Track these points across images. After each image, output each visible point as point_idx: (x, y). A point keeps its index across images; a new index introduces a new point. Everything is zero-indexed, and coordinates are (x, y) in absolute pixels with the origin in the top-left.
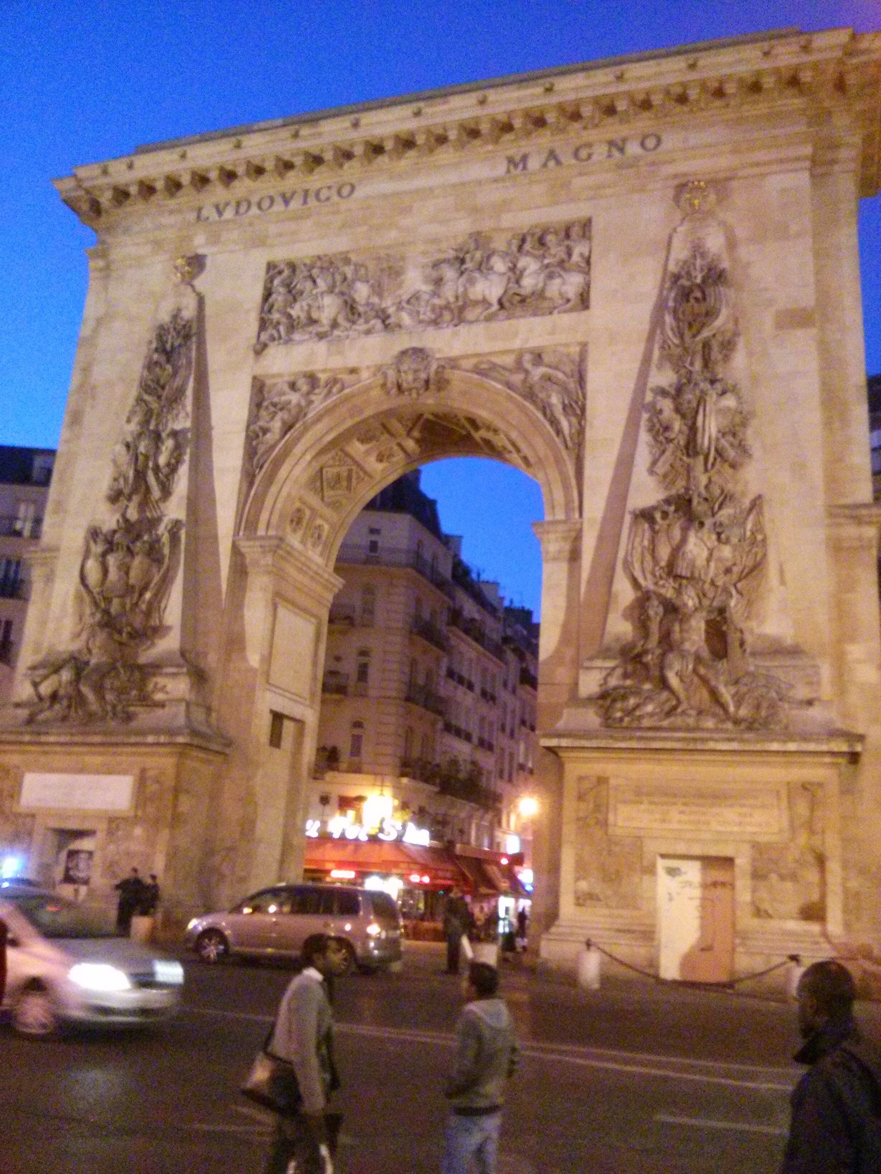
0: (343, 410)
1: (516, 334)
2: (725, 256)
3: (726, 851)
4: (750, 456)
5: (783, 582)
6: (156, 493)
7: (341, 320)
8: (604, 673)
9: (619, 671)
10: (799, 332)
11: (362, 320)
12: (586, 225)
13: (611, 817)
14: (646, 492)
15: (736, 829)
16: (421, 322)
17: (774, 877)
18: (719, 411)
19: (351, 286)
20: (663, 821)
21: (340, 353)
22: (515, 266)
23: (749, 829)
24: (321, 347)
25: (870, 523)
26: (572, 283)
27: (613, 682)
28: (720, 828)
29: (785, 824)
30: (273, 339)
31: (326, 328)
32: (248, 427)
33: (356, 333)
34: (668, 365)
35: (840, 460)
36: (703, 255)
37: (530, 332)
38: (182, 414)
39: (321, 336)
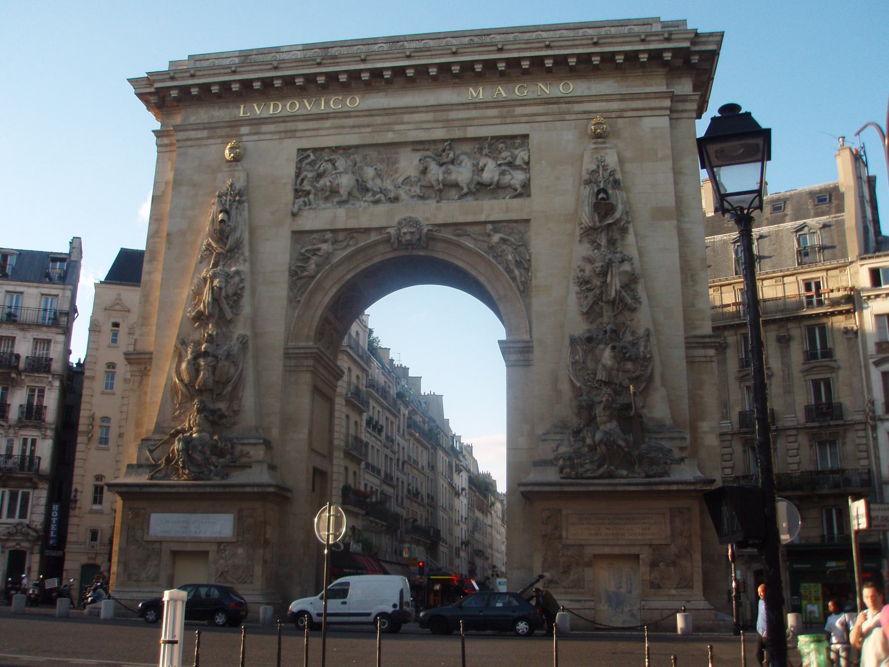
2: (618, 169)
3: (635, 550)
4: (640, 303)
6: (229, 315)
7: (356, 193)
8: (556, 444)
11: (370, 194)
12: (526, 137)
13: (564, 534)
15: (640, 537)
16: (413, 197)
17: (662, 565)
18: (620, 274)
19: (361, 168)
20: (597, 534)
22: (478, 163)
23: (648, 537)
24: (341, 212)
25: (710, 347)
26: (518, 177)
28: (631, 537)
29: (669, 532)
30: (305, 204)
31: (345, 197)
32: (290, 268)
33: (366, 204)
34: (585, 240)
36: (605, 168)
37: (492, 209)
38: (242, 258)
39: (342, 203)
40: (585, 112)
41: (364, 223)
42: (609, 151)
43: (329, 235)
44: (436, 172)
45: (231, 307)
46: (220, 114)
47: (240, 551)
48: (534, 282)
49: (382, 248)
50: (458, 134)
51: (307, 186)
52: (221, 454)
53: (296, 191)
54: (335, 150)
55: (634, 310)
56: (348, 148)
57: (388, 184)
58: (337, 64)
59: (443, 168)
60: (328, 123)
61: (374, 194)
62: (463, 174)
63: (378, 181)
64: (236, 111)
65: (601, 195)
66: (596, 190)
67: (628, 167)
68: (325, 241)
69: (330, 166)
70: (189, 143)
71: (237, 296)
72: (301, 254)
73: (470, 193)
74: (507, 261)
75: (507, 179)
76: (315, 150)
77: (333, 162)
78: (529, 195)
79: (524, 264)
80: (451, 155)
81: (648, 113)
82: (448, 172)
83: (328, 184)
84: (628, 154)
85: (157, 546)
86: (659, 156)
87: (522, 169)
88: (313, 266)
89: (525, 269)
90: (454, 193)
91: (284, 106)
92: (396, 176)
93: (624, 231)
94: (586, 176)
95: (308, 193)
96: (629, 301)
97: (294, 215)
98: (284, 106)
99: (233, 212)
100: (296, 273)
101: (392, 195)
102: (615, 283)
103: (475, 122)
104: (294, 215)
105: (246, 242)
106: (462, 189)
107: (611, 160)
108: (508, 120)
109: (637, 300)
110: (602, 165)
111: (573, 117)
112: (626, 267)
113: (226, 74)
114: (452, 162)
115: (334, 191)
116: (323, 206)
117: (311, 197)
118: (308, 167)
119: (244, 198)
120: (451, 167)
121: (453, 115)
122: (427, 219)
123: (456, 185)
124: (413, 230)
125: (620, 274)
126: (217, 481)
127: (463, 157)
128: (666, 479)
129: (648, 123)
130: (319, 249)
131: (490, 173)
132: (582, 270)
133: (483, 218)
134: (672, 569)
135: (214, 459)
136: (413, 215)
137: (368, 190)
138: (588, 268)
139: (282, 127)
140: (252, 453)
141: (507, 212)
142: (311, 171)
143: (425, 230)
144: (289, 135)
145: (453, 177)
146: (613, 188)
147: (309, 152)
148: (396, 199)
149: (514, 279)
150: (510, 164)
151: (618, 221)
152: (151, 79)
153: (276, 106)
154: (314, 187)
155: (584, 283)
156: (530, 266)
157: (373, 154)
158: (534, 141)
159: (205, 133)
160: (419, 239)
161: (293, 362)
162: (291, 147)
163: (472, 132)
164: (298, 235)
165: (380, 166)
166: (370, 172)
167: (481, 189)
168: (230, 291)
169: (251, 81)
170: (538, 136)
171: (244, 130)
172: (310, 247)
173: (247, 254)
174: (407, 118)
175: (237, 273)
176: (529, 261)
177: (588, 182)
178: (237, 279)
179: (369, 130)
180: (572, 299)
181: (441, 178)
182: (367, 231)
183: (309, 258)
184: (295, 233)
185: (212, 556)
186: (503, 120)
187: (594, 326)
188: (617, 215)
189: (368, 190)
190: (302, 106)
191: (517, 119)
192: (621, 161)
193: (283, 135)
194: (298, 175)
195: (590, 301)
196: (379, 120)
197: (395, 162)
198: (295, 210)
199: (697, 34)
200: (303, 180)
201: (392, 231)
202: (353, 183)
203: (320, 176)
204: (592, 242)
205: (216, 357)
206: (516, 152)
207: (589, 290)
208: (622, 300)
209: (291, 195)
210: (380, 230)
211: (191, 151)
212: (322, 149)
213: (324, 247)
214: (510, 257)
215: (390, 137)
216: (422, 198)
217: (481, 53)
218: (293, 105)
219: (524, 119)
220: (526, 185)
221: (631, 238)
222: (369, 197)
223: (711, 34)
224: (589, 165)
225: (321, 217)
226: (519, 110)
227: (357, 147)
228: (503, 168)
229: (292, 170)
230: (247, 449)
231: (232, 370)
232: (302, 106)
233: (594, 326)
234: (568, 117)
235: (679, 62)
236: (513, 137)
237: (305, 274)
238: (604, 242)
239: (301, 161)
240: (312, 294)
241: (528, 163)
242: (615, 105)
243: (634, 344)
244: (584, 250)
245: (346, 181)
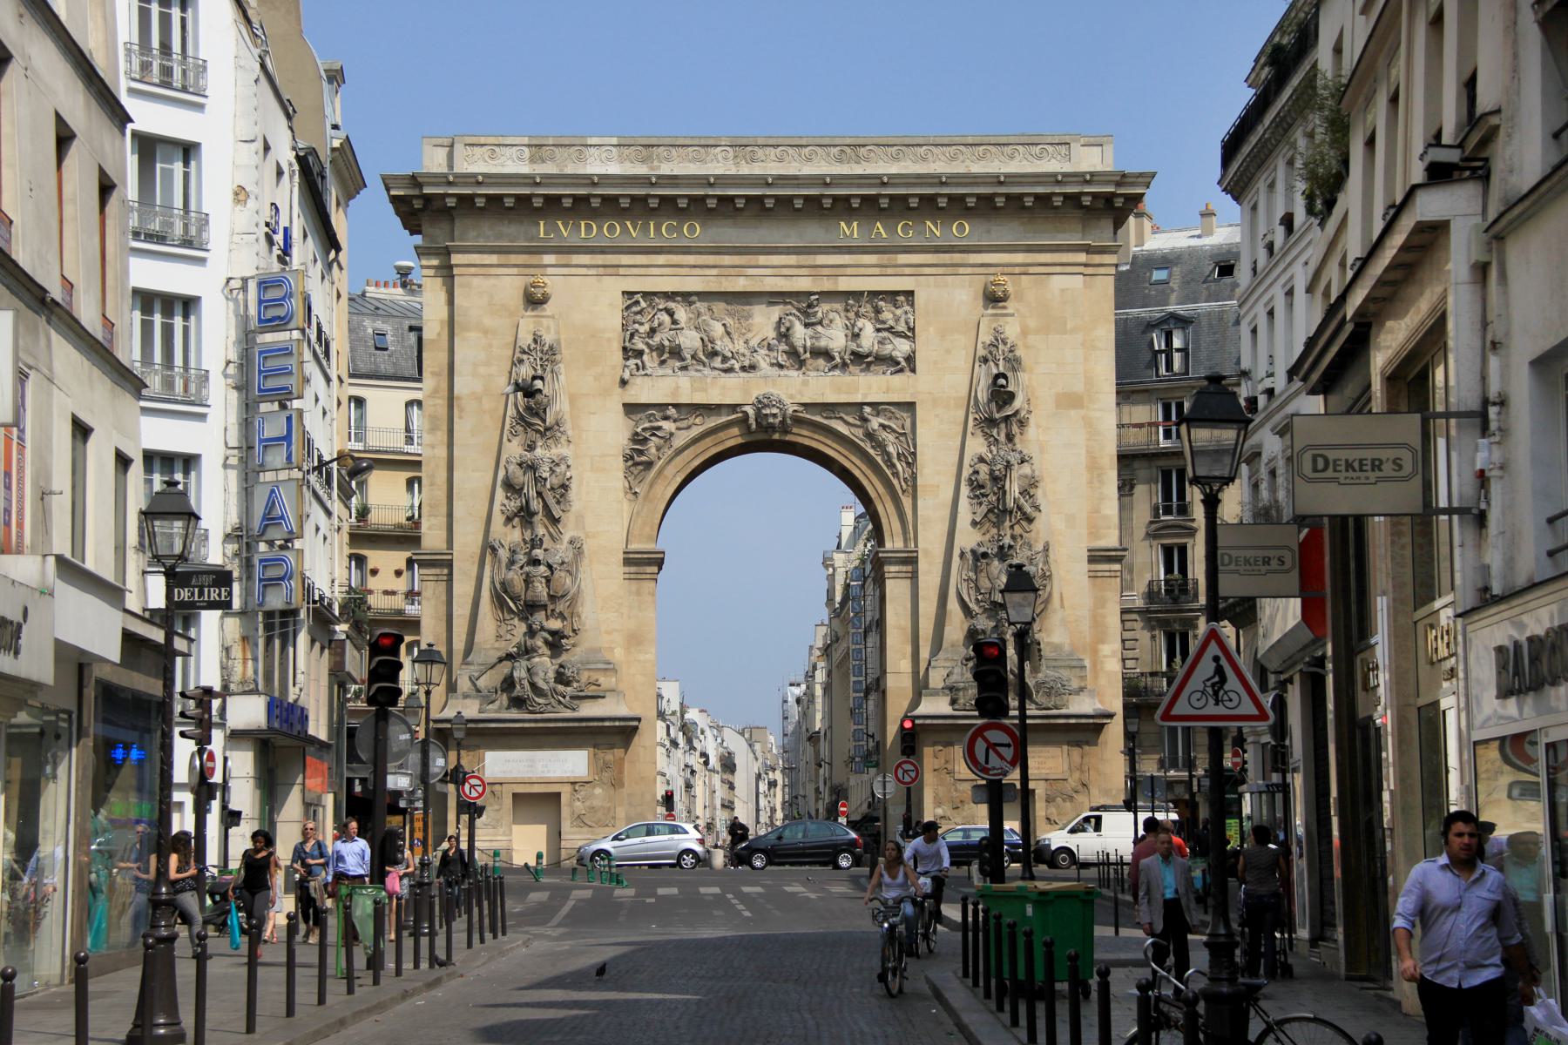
0: (708, 441)
1: (857, 390)
5: (1062, 606)
6: (557, 513)
9: (957, 670)
10: (1073, 413)
11: (719, 359)
12: (911, 293)
14: (968, 538)
16: (772, 365)
21: (705, 390)
22: (853, 326)
27: (954, 678)
29: (1066, 766)
34: (979, 432)
35: (1098, 511)
40: (982, 265)
41: (715, 399)
42: (1009, 319)
43: (672, 411)
44: (800, 334)
45: (558, 502)
46: (513, 232)
47: (598, 791)
48: (919, 481)
49: (735, 431)
50: (827, 285)
51: (641, 346)
52: (567, 683)
53: (625, 349)
54: (670, 296)
55: (1030, 520)
56: (690, 294)
57: (739, 346)
58: (676, 186)
59: (810, 331)
60: (661, 259)
61: (725, 359)
62: (835, 338)
63: (726, 339)
64: (534, 229)
65: (1002, 381)
66: (995, 371)
67: (1031, 339)
68: (666, 418)
69: (666, 318)
70: (473, 270)
71: (565, 487)
72: (637, 434)
73: (844, 366)
74: (889, 454)
75: (887, 349)
76: (646, 295)
77: (671, 313)
78: (913, 371)
79: (910, 458)
80: (820, 315)
81: (1058, 269)
82: (816, 337)
83: (666, 343)
84: (1032, 323)
85: (497, 787)
86: (1069, 326)
87: (906, 337)
88: (653, 450)
89: (908, 464)
90: (821, 362)
91: (600, 228)
92: (749, 335)
93: (1022, 424)
94: (981, 352)
95: (640, 354)
96: (1028, 509)
97: (623, 383)
98: (600, 228)
99: (548, 377)
100: (632, 458)
101: (747, 363)
102: (1014, 489)
103: (849, 271)
104: (623, 383)
105: (567, 417)
106: (833, 358)
107: (1011, 330)
108: (889, 271)
109: (1037, 508)
110: (998, 340)
111: (969, 270)
112: (1026, 469)
113: (526, 185)
114: (820, 323)
115: (676, 353)
116: (661, 372)
117: (645, 357)
118: (638, 317)
119: (558, 357)
120: (819, 328)
121: (822, 259)
122: (791, 397)
123: (826, 354)
124: (775, 411)
125: (1021, 477)
126: (568, 714)
127: (832, 315)
128: (1064, 711)
129: (1058, 282)
130: (659, 428)
131: (869, 340)
132: (977, 472)
133: (859, 400)
134: (1068, 804)
135: (560, 688)
136: (775, 391)
137: (714, 354)
138: (984, 469)
139: (599, 259)
140: (602, 680)
141: (887, 391)
142: (642, 324)
143: (790, 411)
144: (610, 271)
145: (823, 343)
146: (1014, 370)
147: (638, 297)
148: (753, 367)
149: (896, 474)
150: (890, 329)
151: (1017, 412)
152: (414, 180)
153: (589, 227)
154: (647, 344)
155: (976, 486)
156: (915, 459)
157: (719, 307)
158: (919, 299)
159: (493, 259)
160: (783, 422)
161: (633, 569)
162: (614, 287)
163: (845, 284)
164: (631, 409)
165: (729, 321)
166: (717, 329)
167: (859, 359)
168: (556, 481)
169: (559, 198)
170: (926, 292)
171: (549, 259)
172: (647, 425)
173: (570, 433)
174: (762, 260)
175: (564, 459)
176: (914, 454)
177: (985, 360)
178: (563, 467)
179: (714, 272)
180: (964, 503)
181: (808, 344)
182: (719, 406)
183: (646, 440)
184: (625, 405)
185: (564, 799)
186: (883, 270)
187: (988, 536)
188: (1018, 403)
189: (714, 354)
190: (625, 230)
191: (899, 271)
192: (1025, 332)
193: (601, 271)
194: (624, 327)
195: (984, 509)
196: (727, 260)
197: (749, 316)
198: (627, 376)
199: (1124, 176)
200: (632, 336)
201: (750, 411)
202: (698, 344)
203: (653, 331)
204: (987, 436)
205: (550, 567)
206: (898, 312)
207: (983, 495)
208: (1020, 508)
209: (620, 353)
210: (733, 408)
211: (475, 281)
212: (655, 294)
213: (668, 426)
214: (891, 449)
215: (740, 285)
216: (781, 366)
217: (860, 186)
218: (611, 229)
219: (908, 271)
220: (910, 359)
221: (1032, 431)
222: (717, 363)
223: (1141, 175)
224: (985, 337)
225: (661, 385)
226: (903, 258)
227: (698, 294)
228: (885, 334)
229: (618, 322)
230: (595, 676)
231: (568, 581)
232: (625, 230)
233: (988, 536)
234: (962, 270)
235: (1100, 204)
236: (897, 293)
237: (644, 458)
238: (1002, 438)
239: (628, 308)
240: (651, 486)
241: (912, 330)
242: (1019, 258)
243: (1031, 560)
244: (977, 445)
245: (689, 340)
